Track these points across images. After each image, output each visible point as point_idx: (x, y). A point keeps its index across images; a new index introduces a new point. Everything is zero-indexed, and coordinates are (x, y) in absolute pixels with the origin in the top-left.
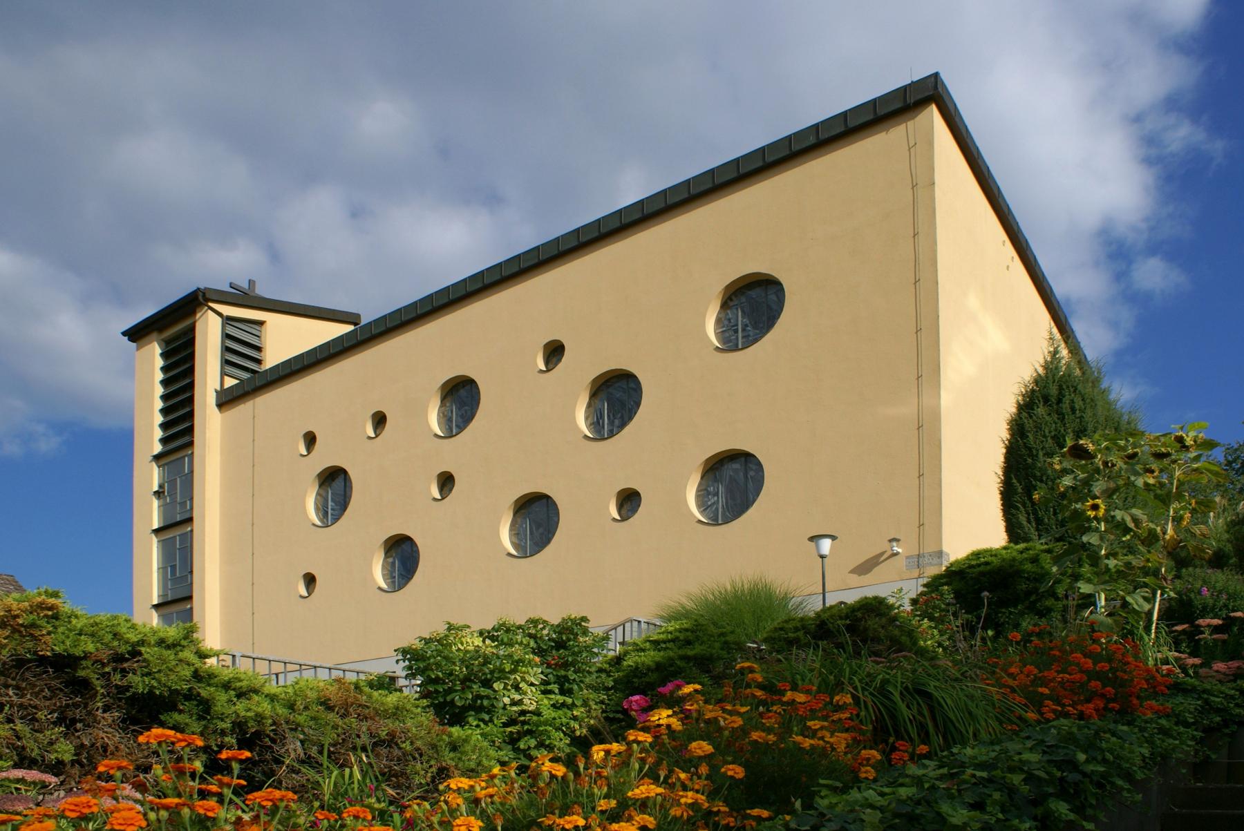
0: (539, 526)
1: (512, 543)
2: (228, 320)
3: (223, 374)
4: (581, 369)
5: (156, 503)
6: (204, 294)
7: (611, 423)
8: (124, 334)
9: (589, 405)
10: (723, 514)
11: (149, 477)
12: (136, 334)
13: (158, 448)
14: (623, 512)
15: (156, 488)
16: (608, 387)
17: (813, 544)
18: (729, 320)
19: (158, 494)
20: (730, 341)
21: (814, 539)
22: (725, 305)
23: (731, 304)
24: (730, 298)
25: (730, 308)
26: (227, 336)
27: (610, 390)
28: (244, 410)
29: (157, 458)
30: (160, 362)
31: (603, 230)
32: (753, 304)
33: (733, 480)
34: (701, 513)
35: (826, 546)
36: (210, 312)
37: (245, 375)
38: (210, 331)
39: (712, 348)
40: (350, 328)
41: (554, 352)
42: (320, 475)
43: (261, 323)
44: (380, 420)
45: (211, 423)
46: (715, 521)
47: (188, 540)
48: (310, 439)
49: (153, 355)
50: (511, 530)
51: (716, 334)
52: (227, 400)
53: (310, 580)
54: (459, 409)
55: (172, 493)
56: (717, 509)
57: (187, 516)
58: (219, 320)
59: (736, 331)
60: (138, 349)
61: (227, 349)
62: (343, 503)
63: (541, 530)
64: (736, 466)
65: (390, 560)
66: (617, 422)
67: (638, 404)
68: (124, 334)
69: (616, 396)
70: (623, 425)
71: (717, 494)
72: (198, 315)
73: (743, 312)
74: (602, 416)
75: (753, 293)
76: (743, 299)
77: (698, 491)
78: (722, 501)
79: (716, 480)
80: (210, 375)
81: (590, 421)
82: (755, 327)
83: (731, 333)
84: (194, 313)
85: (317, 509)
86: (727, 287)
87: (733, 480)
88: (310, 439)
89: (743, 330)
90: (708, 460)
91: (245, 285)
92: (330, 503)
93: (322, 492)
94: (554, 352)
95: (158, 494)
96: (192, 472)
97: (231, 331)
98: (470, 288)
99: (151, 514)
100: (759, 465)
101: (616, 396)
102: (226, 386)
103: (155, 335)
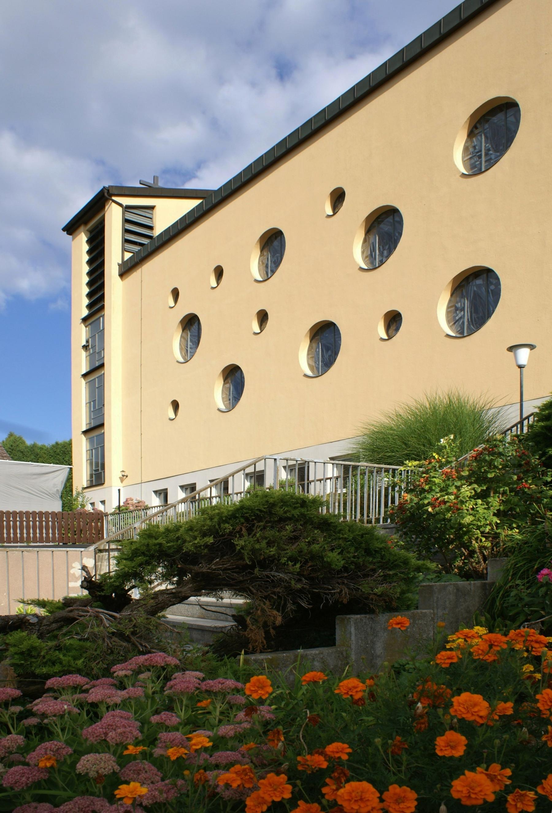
0: (328, 349)
1: (309, 365)
2: (127, 208)
3: (124, 250)
4: (357, 209)
5: (84, 354)
6: (108, 190)
7: (381, 254)
8: (64, 230)
9: (365, 241)
10: (468, 327)
11: (80, 334)
12: (71, 228)
13: (85, 312)
14: (390, 332)
15: (84, 343)
16: (379, 223)
17: (511, 354)
18: (474, 147)
19: (85, 347)
20: (475, 167)
21: (512, 349)
22: (471, 134)
23: (476, 132)
24: (475, 127)
25: (475, 136)
26: (126, 221)
27: (382, 226)
28: (135, 275)
29: (85, 320)
30: (86, 247)
31: (372, 84)
32: (494, 126)
33: (476, 294)
34: (451, 327)
35: (524, 355)
36: (113, 204)
37: (136, 248)
38: (114, 217)
39: (458, 176)
40: (197, 202)
41: (338, 197)
42: (182, 322)
43: (152, 208)
44: (219, 272)
45: (115, 286)
46: (462, 334)
47: (102, 379)
48: (176, 293)
49: (81, 243)
50: (308, 354)
51: (464, 162)
52: (126, 270)
53: (176, 405)
54: (273, 256)
55: (93, 347)
56: (463, 323)
57: (101, 363)
58: (120, 209)
59: (480, 157)
60: (73, 239)
61: (126, 231)
62: (196, 340)
63: (330, 352)
64: (479, 282)
65: (227, 385)
66: (385, 253)
67: (401, 234)
68: (64, 230)
69: (385, 228)
70: (390, 253)
71: (463, 309)
72: (107, 207)
73: (486, 137)
74: (374, 250)
75: (495, 119)
76: (487, 126)
77: (448, 307)
78: (467, 315)
79: (462, 297)
80: (115, 253)
81: (365, 255)
82: (496, 151)
83: (476, 159)
84: (104, 207)
85: (181, 349)
86: (472, 116)
87: (476, 294)
88: (176, 293)
89: (486, 154)
90: (455, 279)
91: (150, 181)
92: (189, 343)
93: (184, 335)
94: (338, 197)
95: (85, 347)
96: (104, 329)
97: (129, 216)
98: (277, 154)
99: (81, 362)
100: (497, 279)
101: (385, 228)
102: (126, 258)
103: (82, 228)
